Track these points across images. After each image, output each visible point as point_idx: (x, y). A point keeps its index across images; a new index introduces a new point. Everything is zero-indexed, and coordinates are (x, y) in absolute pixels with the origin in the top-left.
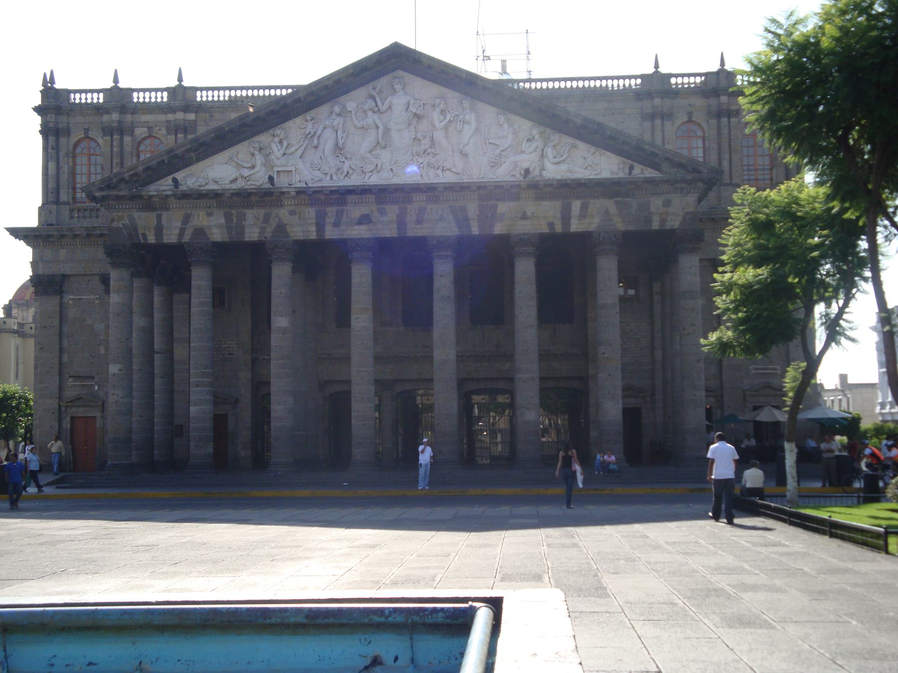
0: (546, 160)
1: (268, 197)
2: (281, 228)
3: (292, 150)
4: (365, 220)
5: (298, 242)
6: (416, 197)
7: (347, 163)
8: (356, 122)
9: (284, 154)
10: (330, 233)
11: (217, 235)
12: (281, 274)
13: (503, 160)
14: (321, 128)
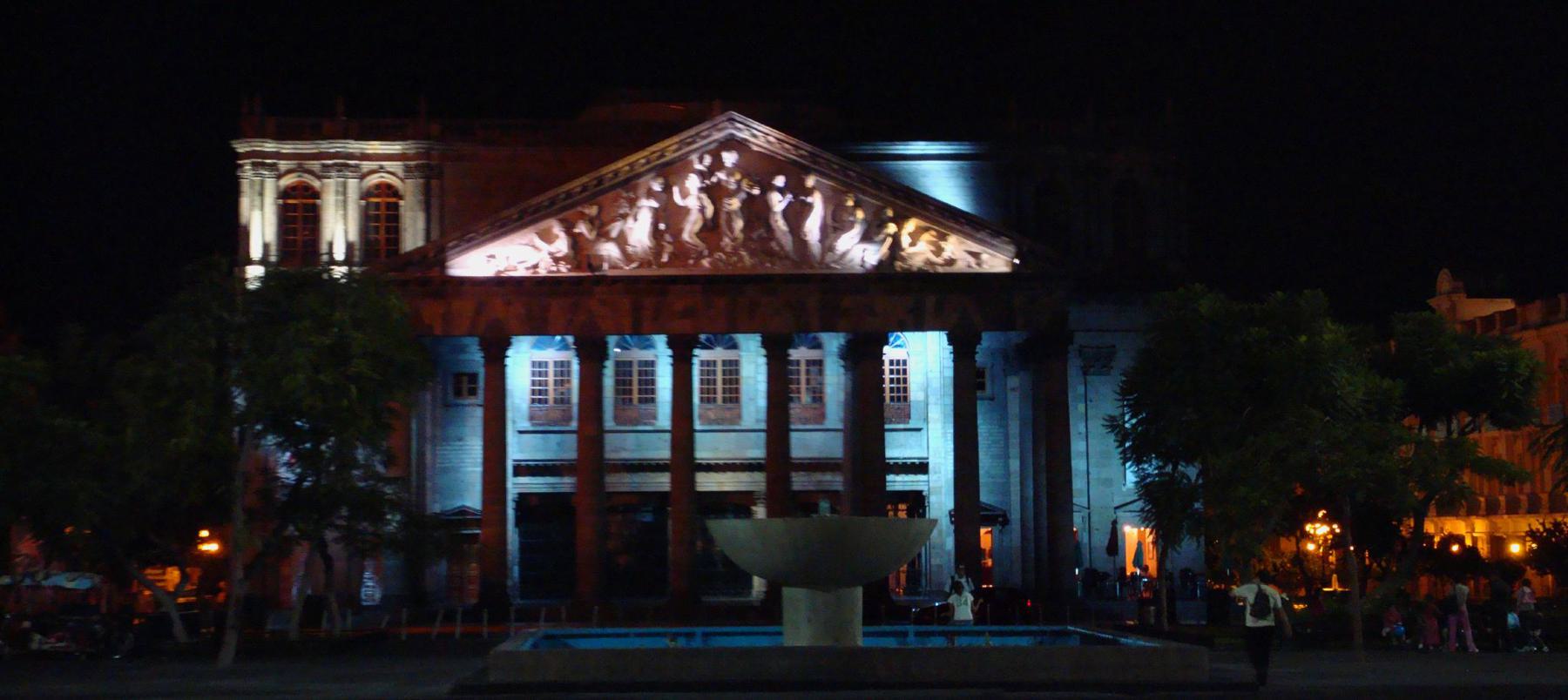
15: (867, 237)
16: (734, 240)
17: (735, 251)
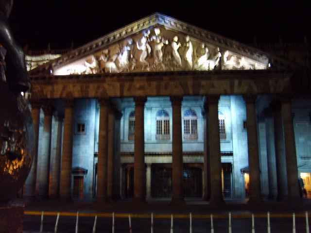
2: (105, 91)
6: (164, 78)
15: (209, 58)
16: (159, 61)
17: (160, 64)
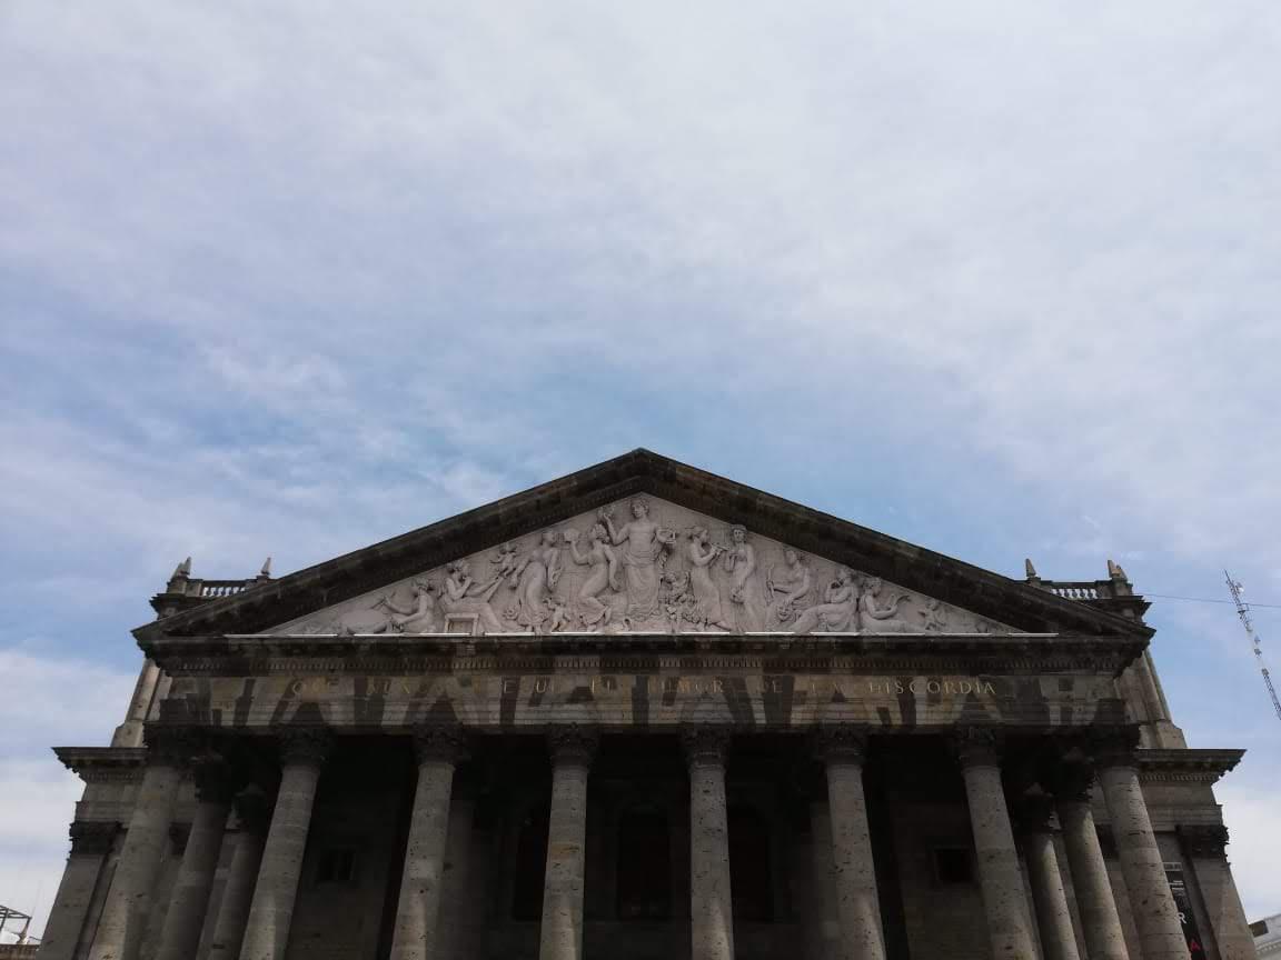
0: (865, 615)
1: (432, 655)
2: (444, 705)
3: (478, 590)
4: (582, 695)
5: (466, 730)
6: (666, 661)
7: (560, 611)
8: (577, 555)
9: (463, 597)
10: (524, 716)
11: (339, 715)
12: (434, 787)
13: (798, 611)
14: (524, 562)
